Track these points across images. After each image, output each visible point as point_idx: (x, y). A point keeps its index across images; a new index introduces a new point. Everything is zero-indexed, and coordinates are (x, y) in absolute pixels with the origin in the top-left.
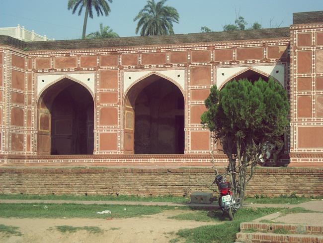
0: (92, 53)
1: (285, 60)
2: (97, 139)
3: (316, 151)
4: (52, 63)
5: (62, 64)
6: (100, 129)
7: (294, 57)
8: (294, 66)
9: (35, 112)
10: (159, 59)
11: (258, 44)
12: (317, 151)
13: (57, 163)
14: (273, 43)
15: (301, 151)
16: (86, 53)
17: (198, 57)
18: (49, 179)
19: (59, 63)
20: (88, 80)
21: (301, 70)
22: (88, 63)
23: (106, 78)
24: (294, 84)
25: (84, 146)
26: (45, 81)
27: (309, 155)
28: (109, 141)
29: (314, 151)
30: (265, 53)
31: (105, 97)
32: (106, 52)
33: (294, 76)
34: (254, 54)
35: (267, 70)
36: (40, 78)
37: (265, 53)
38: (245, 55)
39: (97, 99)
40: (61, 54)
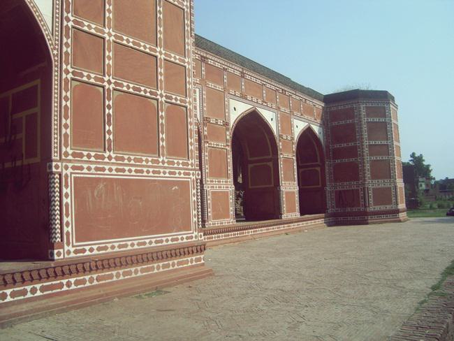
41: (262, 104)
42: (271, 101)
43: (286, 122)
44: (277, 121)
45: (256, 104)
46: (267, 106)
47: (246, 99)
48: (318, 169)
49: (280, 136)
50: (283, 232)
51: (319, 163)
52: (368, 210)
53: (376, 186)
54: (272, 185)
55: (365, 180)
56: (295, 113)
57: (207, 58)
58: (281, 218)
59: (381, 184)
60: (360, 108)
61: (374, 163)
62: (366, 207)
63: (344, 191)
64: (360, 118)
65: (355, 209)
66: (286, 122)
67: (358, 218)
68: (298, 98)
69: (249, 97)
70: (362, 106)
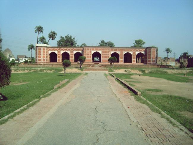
0: (57, 48)
1: (83, 51)
2: (57, 60)
4: (51, 50)
5: (52, 50)
6: (58, 59)
7: (84, 51)
8: (84, 52)
9: (49, 56)
10: (66, 50)
11: (79, 49)
13: (52, 63)
14: (81, 48)
16: (56, 48)
17: (71, 50)
18: (56, 65)
19: (52, 50)
20: (56, 52)
21: (85, 53)
22: (56, 50)
23: (59, 52)
24: (84, 54)
25: (55, 61)
26: (50, 52)
28: (59, 60)
30: (80, 50)
31: (58, 54)
32: (59, 49)
33: (84, 53)
34: (79, 50)
35: (80, 52)
36: (49, 52)
37: (80, 50)
38: (77, 50)
39: (57, 55)
40: (52, 48)
43: (134, 53)
59: (150, 59)
61: (149, 57)
66: (134, 53)
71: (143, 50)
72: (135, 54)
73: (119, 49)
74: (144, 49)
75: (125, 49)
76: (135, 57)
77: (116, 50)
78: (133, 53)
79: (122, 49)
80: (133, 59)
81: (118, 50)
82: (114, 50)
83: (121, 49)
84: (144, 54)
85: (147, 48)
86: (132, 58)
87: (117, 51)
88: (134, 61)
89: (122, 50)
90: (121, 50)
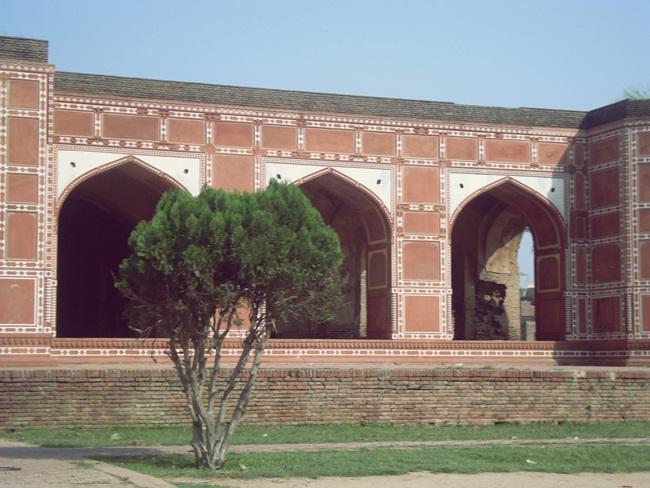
3: (24, 332)
12: (7, 330)
15: (14, 330)
27: (47, 340)
29: (21, 330)
41: (351, 161)
42: (380, 151)
43: (421, 185)
44: (395, 183)
45: (331, 163)
46: (365, 161)
47: (308, 158)
48: (557, 256)
49: (401, 208)
50: (387, 360)
51: (558, 246)
52: (631, 337)
53: (415, 292)
54: (385, 286)
55: (627, 280)
56: (455, 163)
57: (219, 114)
58: (390, 338)
60: (626, 137)
62: (627, 332)
63: (603, 300)
64: (625, 157)
65: (615, 336)
66: (421, 185)
67: (617, 354)
68: (471, 134)
69: (313, 156)
70: (630, 132)
71: (546, 156)
72: (440, 209)
73: (194, 112)
74: (561, 137)
75: (288, 119)
76: (434, 249)
77: (142, 129)
78: (409, 195)
79: (242, 115)
80: (403, 289)
81: (178, 128)
82: (118, 129)
83: (227, 114)
84: (559, 203)
85: (593, 121)
86: (397, 267)
87: (159, 146)
88: (422, 314)
89: (246, 131)
90: (225, 132)
